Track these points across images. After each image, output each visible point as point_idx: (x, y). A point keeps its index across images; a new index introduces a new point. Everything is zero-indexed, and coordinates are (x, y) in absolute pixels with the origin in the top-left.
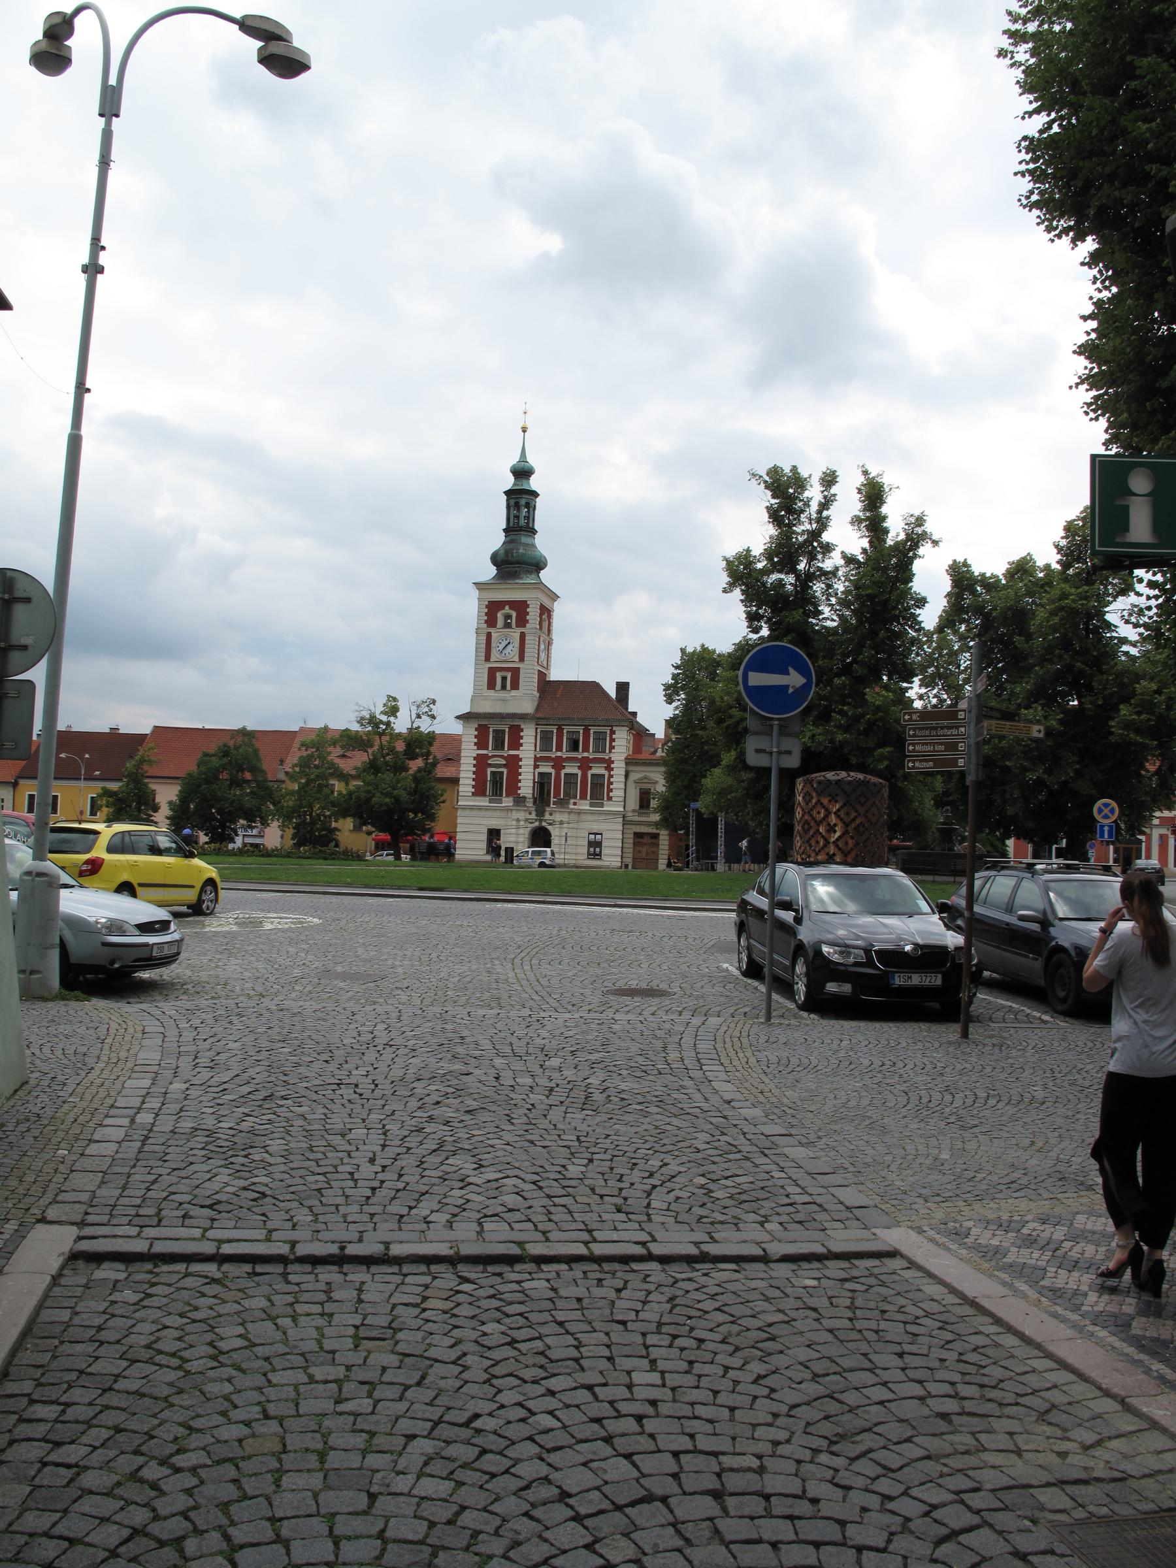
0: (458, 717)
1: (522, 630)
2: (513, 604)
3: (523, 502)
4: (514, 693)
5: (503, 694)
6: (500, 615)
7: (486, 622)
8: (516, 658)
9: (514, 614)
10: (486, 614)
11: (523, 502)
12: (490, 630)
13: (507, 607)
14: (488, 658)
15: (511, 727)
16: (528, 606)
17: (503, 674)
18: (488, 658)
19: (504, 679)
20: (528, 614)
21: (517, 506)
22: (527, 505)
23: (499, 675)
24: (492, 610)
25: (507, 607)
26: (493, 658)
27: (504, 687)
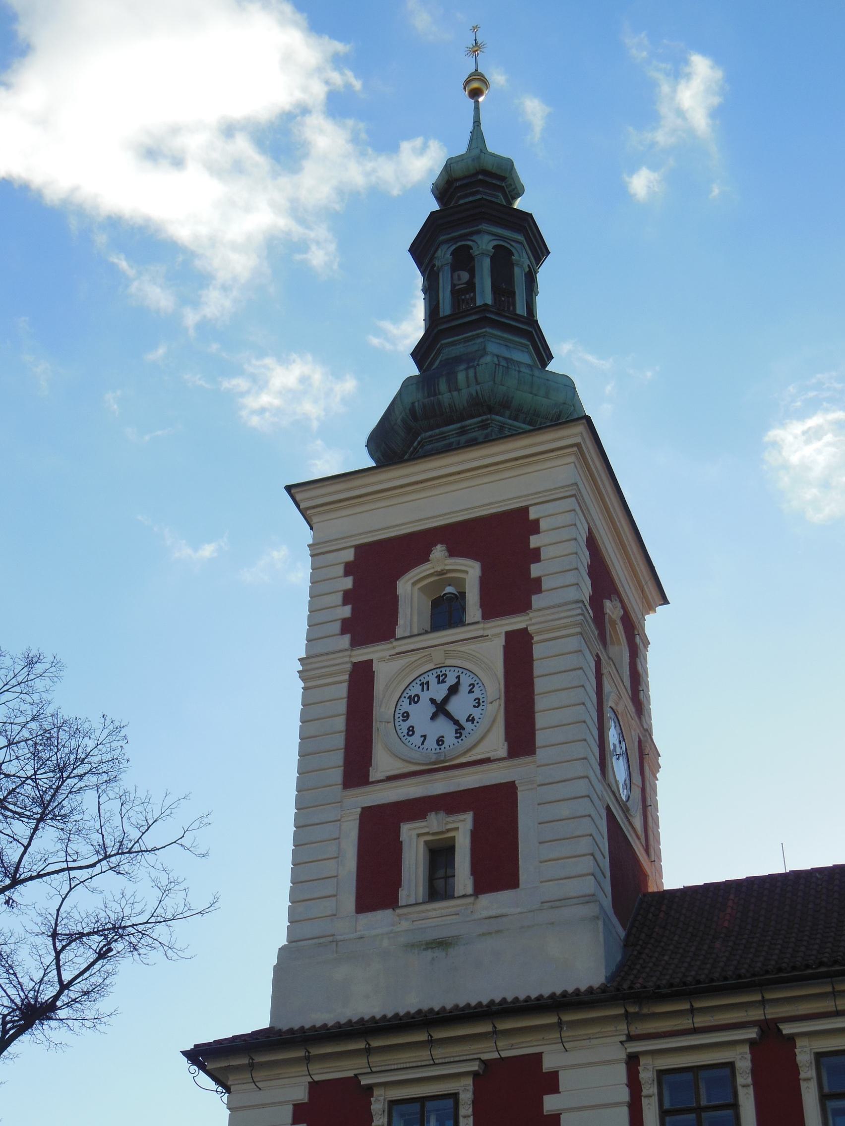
0: (200, 1056)
1: (516, 623)
2: (461, 537)
3: (484, 244)
4: (493, 903)
5: (439, 917)
6: (411, 590)
7: (347, 626)
8: (495, 743)
9: (471, 572)
10: (348, 597)
11: (484, 244)
12: (362, 654)
13: (439, 552)
14: (357, 771)
15: (488, 1076)
16: (534, 527)
17: (435, 823)
18: (357, 771)
19: (440, 855)
20: (535, 555)
21: (464, 260)
22: (502, 259)
23: (413, 839)
24: (367, 590)
25: (439, 552)
26: (383, 763)
27: (438, 888)
